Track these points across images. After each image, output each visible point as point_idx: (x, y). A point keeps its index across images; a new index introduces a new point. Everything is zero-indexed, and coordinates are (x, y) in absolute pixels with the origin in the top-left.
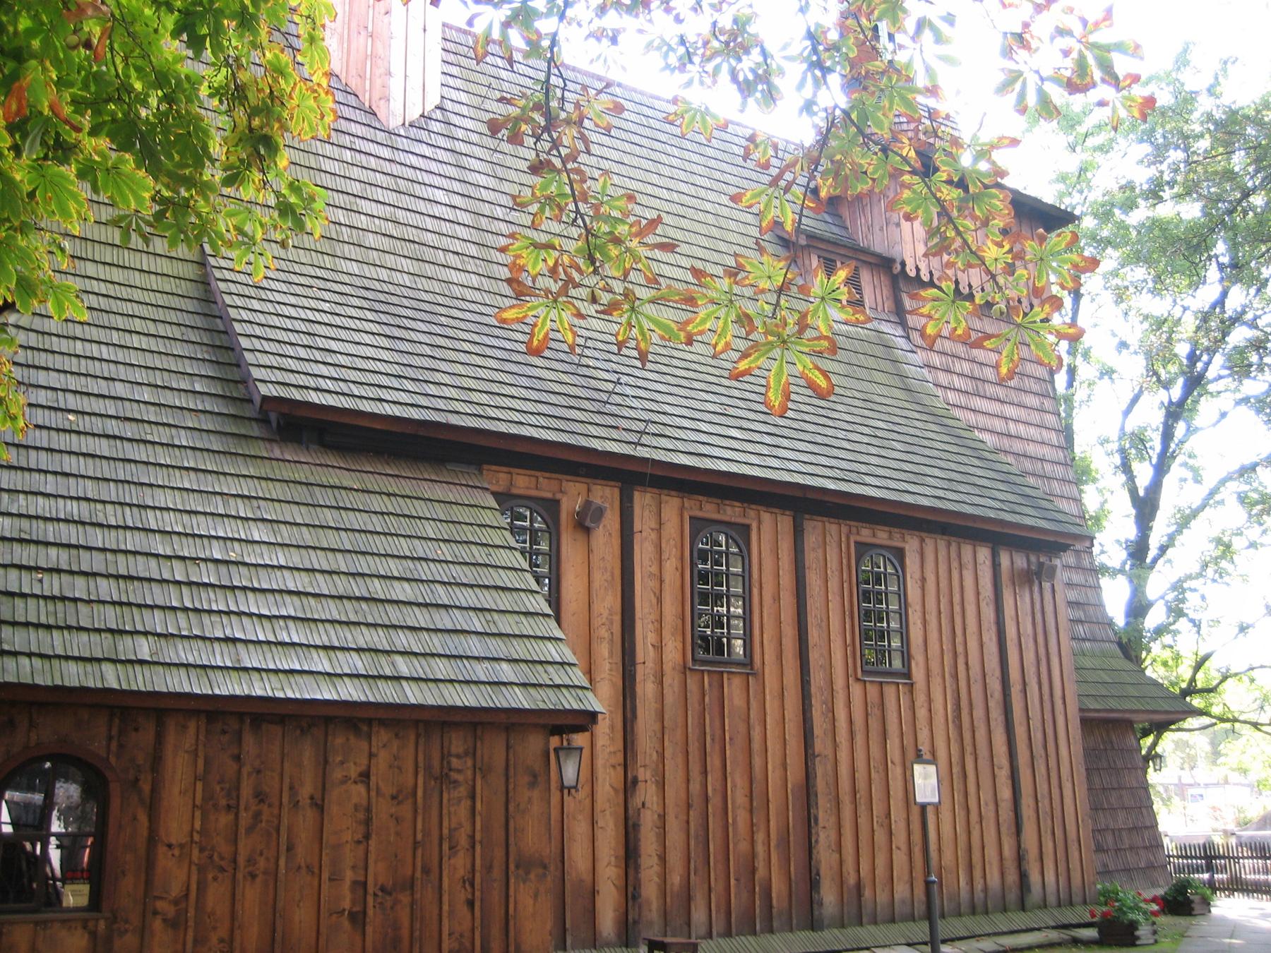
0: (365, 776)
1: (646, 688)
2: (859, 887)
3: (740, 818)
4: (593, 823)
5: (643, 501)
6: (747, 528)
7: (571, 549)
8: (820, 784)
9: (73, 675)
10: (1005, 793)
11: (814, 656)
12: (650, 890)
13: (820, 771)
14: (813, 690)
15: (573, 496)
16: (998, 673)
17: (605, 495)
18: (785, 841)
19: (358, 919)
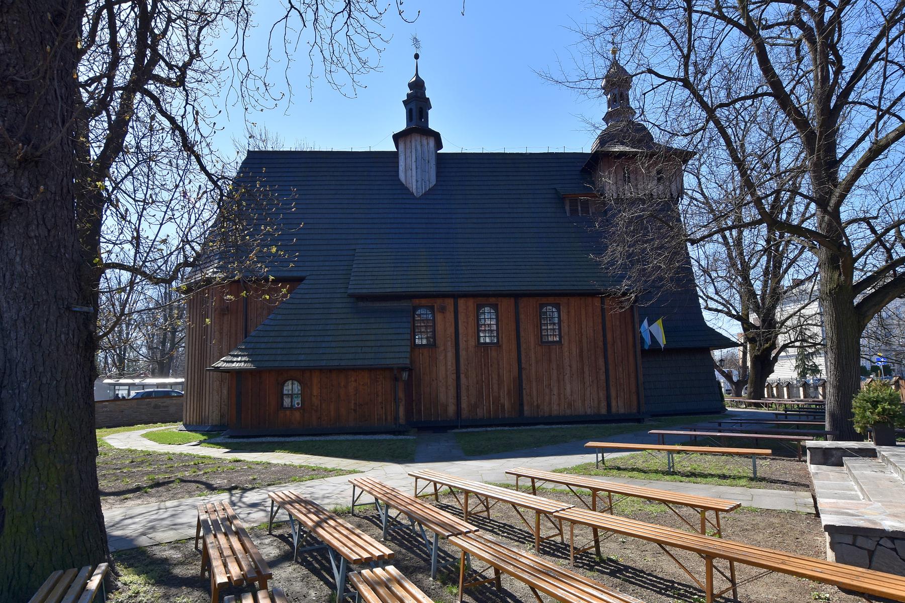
0: (356, 381)
1: (463, 353)
2: (538, 406)
3: (496, 387)
4: (447, 388)
5: (461, 302)
6: (497, 305)
7: (439, 317)
8: (524, 377)
9: (293, 364)
10: (603, 377)
11: (522, 340)
12: (464, 405)
13: (524, 372)
14: (522, 349)
15: (439, 302)
16: (602, 339)
17: (449, 302)
18: (509, 393)
19: (355, 410)
